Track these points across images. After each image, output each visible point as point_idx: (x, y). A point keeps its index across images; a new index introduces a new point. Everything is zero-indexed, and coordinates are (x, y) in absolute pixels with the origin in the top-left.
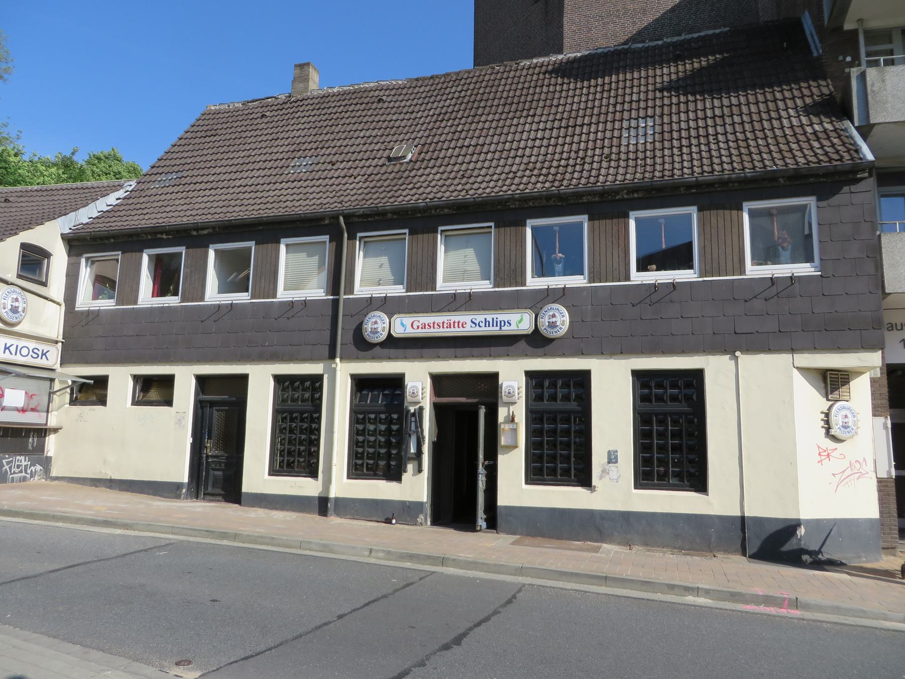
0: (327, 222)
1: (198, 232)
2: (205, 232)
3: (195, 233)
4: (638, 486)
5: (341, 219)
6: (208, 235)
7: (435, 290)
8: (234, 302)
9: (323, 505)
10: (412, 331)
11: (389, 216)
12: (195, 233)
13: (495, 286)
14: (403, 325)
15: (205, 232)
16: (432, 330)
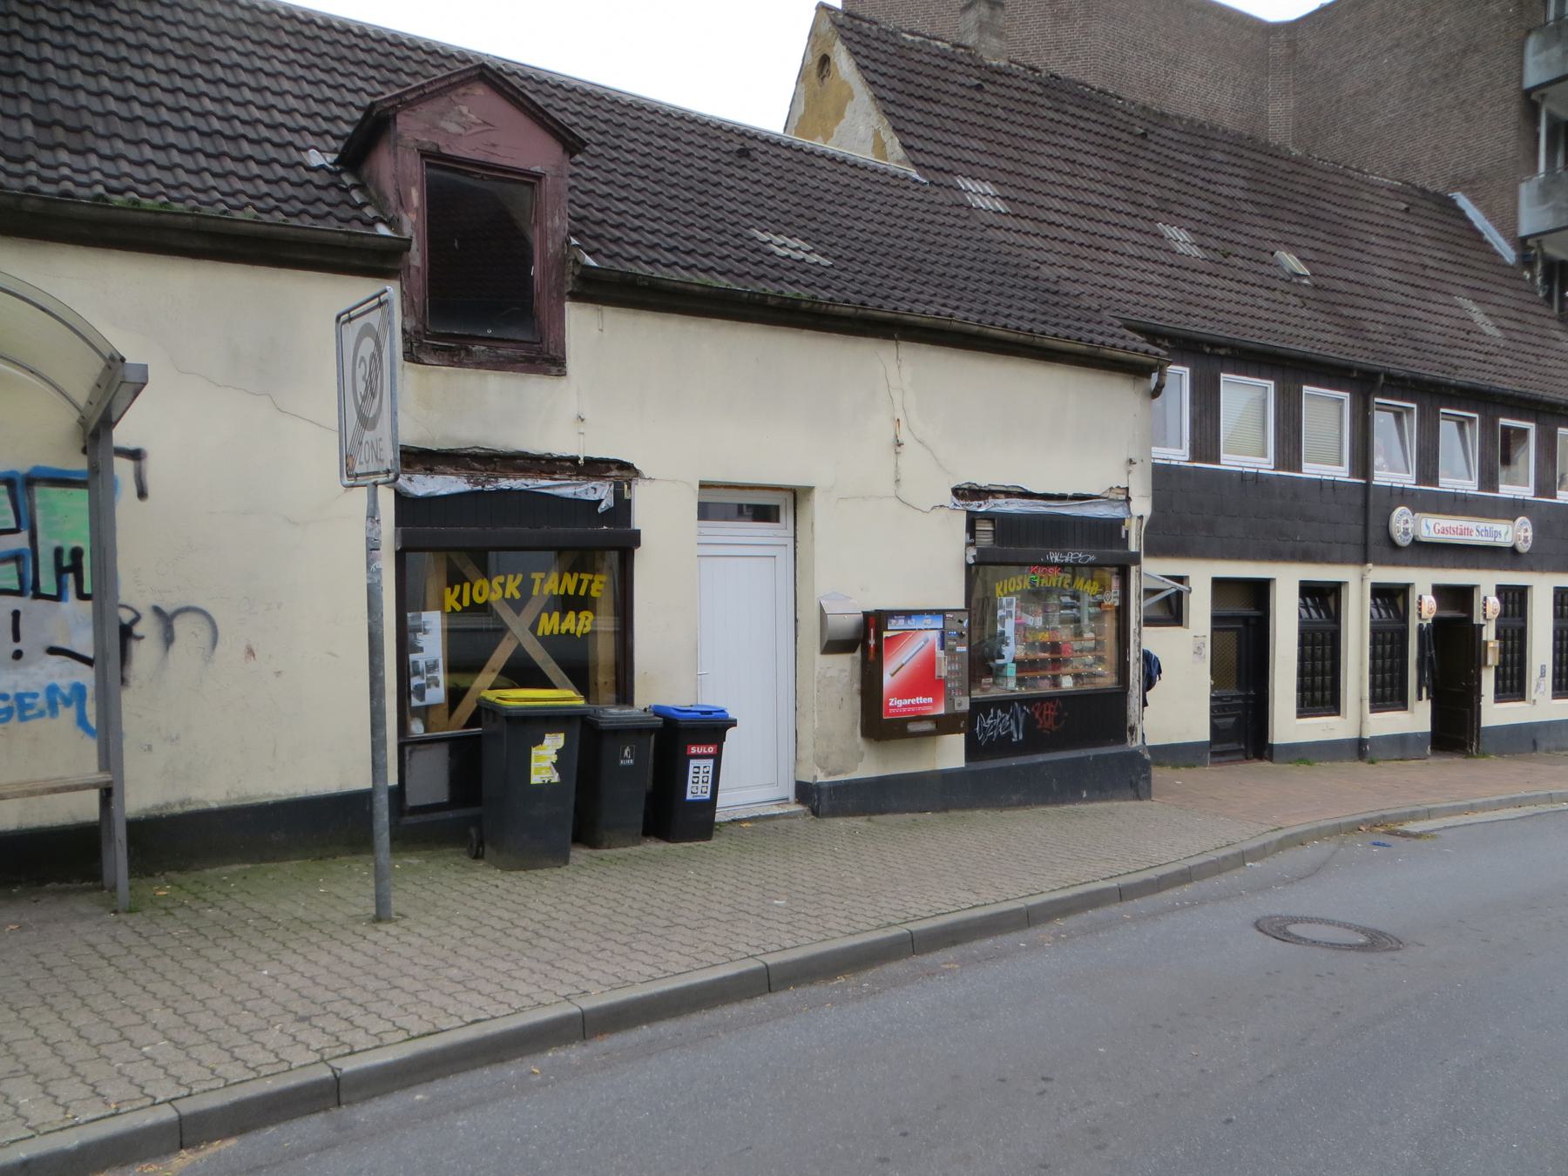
0: (1355, 375)
1: (1212, 349)
2: (1222, 352)
3: (1208, 350)
4: (1555, 697)
5: (1382, 377)
6: (1226, 356)
7: (1437, 485)
8: (1260, 471)
9: (1360, 749)
10: (1435, 535)
11: (1409, 383)
12: (1208, 350)
13: (1479, 490)
14: (1428, 527)
15: (1222, 352)
16: (1449, 536)
